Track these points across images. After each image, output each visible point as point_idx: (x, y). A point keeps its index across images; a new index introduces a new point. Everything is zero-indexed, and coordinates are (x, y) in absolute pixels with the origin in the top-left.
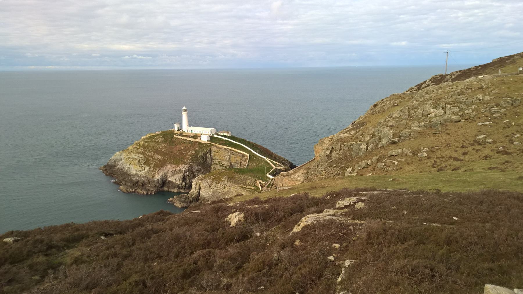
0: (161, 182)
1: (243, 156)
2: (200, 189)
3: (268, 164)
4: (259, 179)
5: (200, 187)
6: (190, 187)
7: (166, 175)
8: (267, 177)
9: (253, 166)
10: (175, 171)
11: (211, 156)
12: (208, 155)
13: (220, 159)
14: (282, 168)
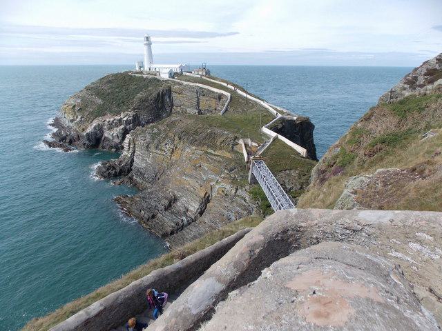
1: (220, 97)
4: (245, 137)
8: (265, 135)
9: (236, 115)
10: (113, 122)
11: (172, 101)
13: (184, 105)
14: (295, 118)
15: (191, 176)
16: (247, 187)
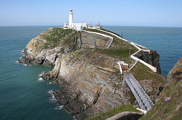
1: (107, 40)
11: (81, 41)
12: (79, 40)
14: (149, 51)
15: (90, 82)
16: (122, 89)
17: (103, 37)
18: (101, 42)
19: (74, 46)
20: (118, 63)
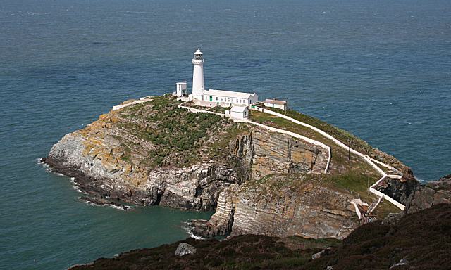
0: (153, 194)
1: (317, 151)
2: (233, 211)
3: (372, 167)
5: (235, 207)
6: (213, 207)
7: (163, 182)
12: (247, 147)
14: (400, 177)
17: (308, 143)
18: (304, 154)
19: (237, 161)
20: (352, 202)
